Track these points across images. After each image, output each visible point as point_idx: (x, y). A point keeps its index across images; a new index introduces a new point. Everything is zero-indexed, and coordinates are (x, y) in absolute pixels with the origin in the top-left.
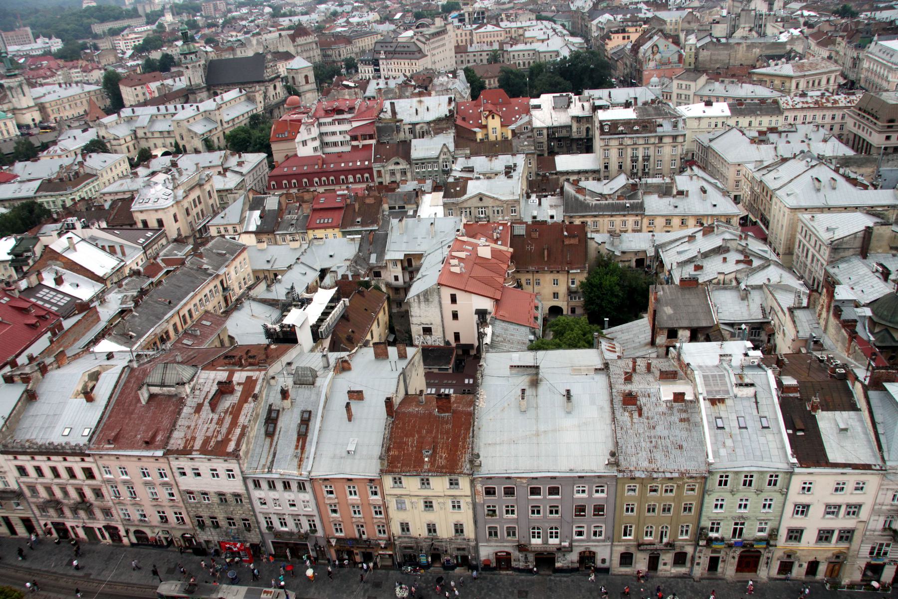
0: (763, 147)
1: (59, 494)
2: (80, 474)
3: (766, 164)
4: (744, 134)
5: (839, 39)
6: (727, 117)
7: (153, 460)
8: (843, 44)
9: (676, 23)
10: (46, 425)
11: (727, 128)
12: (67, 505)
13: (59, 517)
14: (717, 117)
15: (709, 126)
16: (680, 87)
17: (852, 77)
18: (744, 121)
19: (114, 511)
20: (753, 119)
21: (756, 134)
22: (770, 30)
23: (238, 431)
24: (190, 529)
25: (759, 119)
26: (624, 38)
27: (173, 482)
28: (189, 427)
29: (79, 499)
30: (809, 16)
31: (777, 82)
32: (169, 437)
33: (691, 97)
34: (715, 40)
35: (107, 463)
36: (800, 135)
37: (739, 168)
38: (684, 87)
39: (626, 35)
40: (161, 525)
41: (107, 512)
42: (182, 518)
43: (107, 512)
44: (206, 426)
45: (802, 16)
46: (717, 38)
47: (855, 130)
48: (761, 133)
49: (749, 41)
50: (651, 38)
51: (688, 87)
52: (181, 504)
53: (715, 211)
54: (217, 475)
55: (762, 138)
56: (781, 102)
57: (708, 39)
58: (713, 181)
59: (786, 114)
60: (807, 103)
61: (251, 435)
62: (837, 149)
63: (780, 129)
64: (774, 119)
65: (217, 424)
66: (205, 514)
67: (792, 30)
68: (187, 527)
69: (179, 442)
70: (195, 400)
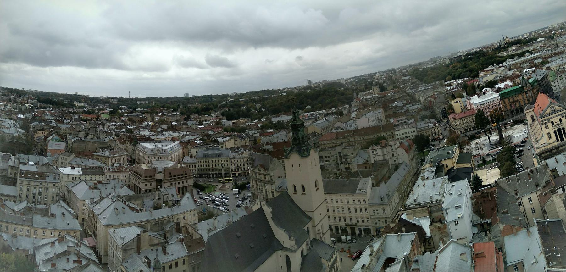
0: (95, 191)
3: (95, 200)
4: (87, 184)
5: (127, 142)
6: (81, 175)
8: (129, 144)
9: (66, 130)
11: (80, 181)
14: (76, 175)
15: (73, 179)
16: (62, 158)
17: (134, 158)
18: (88, 178)
20: (92, 177)
21: (93, 185)
22: (101, 136)
25: (95, 176)
26: (42, 133)
30: (117, 132)
31: (103, 159)
33: (67, 164)
34: (79, 139)
36: (111, 185)
37: (84, 202)
38: (64, 159)
39: (44, 132)
45: (114, 131)
46: (80, 138)
47: (134, 182)
48: (95, 184)
49: (93, 140)
50: (52, 135)
51: (66, 159)
53: (68, 228)
55: (95, 186)
56: (104, 169)
57: (77, 138)
58: (69, 209)
59: (106, 174)
60: (114, 169)
62: (126, 192)
63: (103, 182)
64: (101, 177)
67: (110, 137)
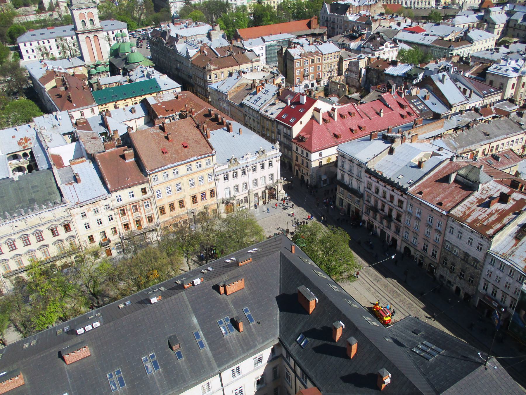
1: (379, 206)
2: (396, 202)
7: (439, 215)
10: (392, 169)
12: (380, 214)
13: (373, 218)
19: (401, 230)
23: (499, 226)
24: (436, 263)
27: (443, 232)
28: (469, 208)
29: (387, 214)
32: (455, 207)
35: (413, 203)
40: (422, 252)
41: (397, 230)
42: (435, 255)
43: (397, 230)
44: (480, 213)
52: (440, 247)
54: (471, 243)
61: (505, 232)
65: (488, 215)
66: (450, 259)
68: (435, 261)
69: (460, 213)
70: (482, 196)
